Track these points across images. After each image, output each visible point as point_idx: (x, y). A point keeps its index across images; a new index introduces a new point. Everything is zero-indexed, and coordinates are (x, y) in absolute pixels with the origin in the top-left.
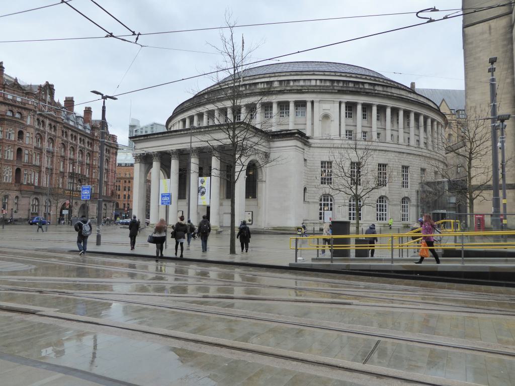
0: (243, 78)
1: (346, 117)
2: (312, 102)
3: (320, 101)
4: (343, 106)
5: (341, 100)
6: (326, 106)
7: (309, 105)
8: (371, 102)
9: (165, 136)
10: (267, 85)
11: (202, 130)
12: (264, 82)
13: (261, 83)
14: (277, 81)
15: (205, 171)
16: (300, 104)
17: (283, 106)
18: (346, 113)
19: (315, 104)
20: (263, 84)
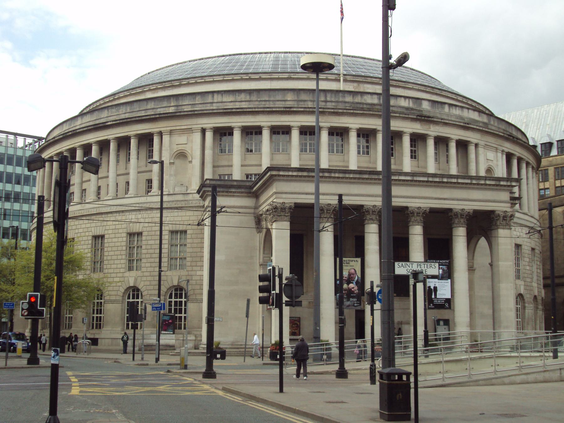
0: (344, 75)
1: (359, 153)
2: (476, 145)
3: (486, 147)
4: (504, 157)
5: (504, 148)
6: (491, 155)
7: (472, 149)
8: (523, 157)
9: (363, 179)
10: (414, 103)
11: (445, 180)
12: (409, 98)
13: (405, 97)
14: (429, 100)
15: (439, 249)
16: (462, 145)
17: (441, 142)
18: (359, 147)
19: (481, 150)
20: (407, 100)
